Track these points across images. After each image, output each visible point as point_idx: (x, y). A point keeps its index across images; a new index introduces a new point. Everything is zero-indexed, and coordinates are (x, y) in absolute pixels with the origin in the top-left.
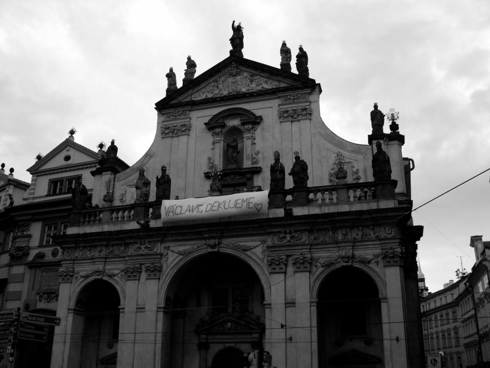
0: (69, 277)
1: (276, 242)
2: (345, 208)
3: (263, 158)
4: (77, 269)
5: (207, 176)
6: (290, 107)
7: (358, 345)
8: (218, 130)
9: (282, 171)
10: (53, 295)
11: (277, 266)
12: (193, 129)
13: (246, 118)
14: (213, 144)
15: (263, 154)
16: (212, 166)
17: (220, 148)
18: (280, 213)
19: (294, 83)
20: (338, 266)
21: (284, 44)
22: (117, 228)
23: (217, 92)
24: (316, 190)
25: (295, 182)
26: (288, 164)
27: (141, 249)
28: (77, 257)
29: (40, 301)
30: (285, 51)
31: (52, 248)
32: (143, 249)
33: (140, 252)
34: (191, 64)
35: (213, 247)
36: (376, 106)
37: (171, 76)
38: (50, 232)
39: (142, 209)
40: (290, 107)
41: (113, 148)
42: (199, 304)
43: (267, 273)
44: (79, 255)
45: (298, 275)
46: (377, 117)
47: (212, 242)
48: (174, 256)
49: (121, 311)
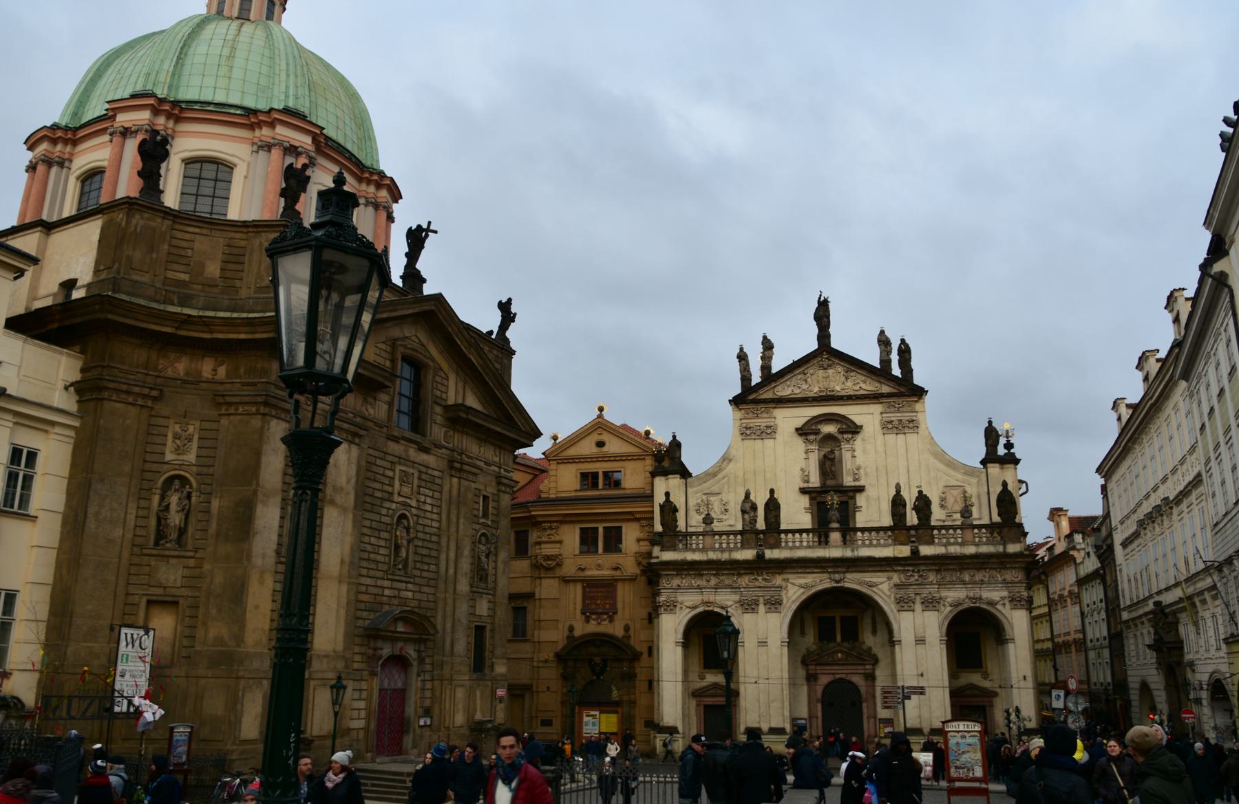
0: (672, 607)
2: (971, 550)
3: (866, 474)
4: (680, 598)
5: (803, 491)
6: (895, 417)
7: (975, 678)
8: (812, 437)
9: (905, 505)
11: (904, 604)
12: (779, 431)
14: (806, 452)
17: (814, 459)
18: (905, 551)
19: (896, 383)
20: (965, 606)
21: (882, 332)
22: (725, 556)
23: (805, 387)
24: (940, 528)
25: (919, 518)
26: (910, 497)
30: (884, 341)
33: (757, 584)
34: (768, 345)
35: (838, 582)
36: (990, 422)
37: (742, 357)
39: (753, 536)
40: (895, 417)
41: (676, 445)
42: (803, 633)
45: (926, 613)
46: (991, 435)
48: (795, 590)
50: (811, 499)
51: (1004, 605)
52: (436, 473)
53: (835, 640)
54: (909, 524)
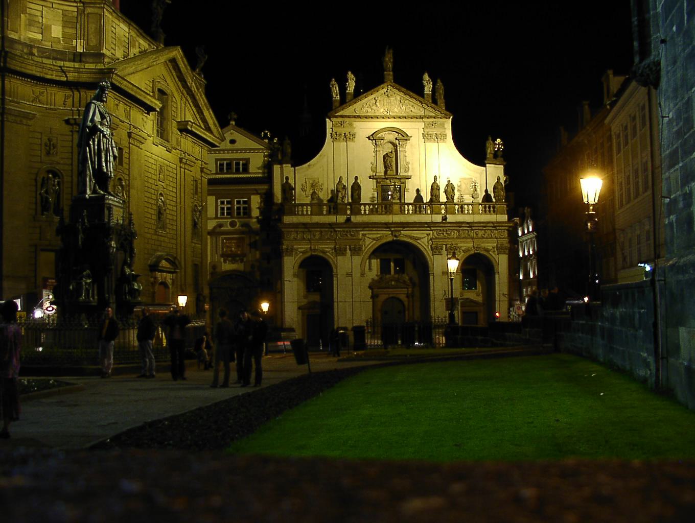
0: (290, 252)
1: (437, 236)
10: (238, 258)
13: (400, 136)
14: (376, 152)
15: (412, 164)
16: (374, 169)
25: (447, 198)
27: (347, 235)
28: (296, 239)
29: (225, 262)
31: (230, 220)
32: (349, 236)
38: (223, 206)
43: (431, 254)
44: (297, 236)
47: (397, 234)
49: (334, 276)
50: (377, 182)
51: (494, 251)
52: (174, 166)
53: (390, 274)
54: (441, 201)
